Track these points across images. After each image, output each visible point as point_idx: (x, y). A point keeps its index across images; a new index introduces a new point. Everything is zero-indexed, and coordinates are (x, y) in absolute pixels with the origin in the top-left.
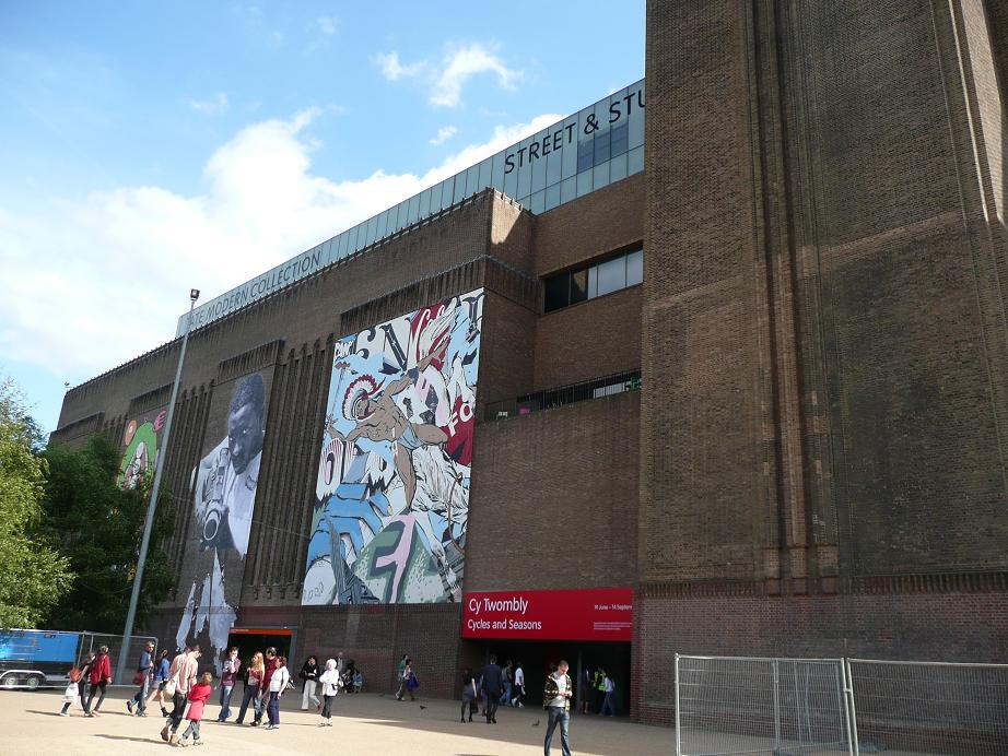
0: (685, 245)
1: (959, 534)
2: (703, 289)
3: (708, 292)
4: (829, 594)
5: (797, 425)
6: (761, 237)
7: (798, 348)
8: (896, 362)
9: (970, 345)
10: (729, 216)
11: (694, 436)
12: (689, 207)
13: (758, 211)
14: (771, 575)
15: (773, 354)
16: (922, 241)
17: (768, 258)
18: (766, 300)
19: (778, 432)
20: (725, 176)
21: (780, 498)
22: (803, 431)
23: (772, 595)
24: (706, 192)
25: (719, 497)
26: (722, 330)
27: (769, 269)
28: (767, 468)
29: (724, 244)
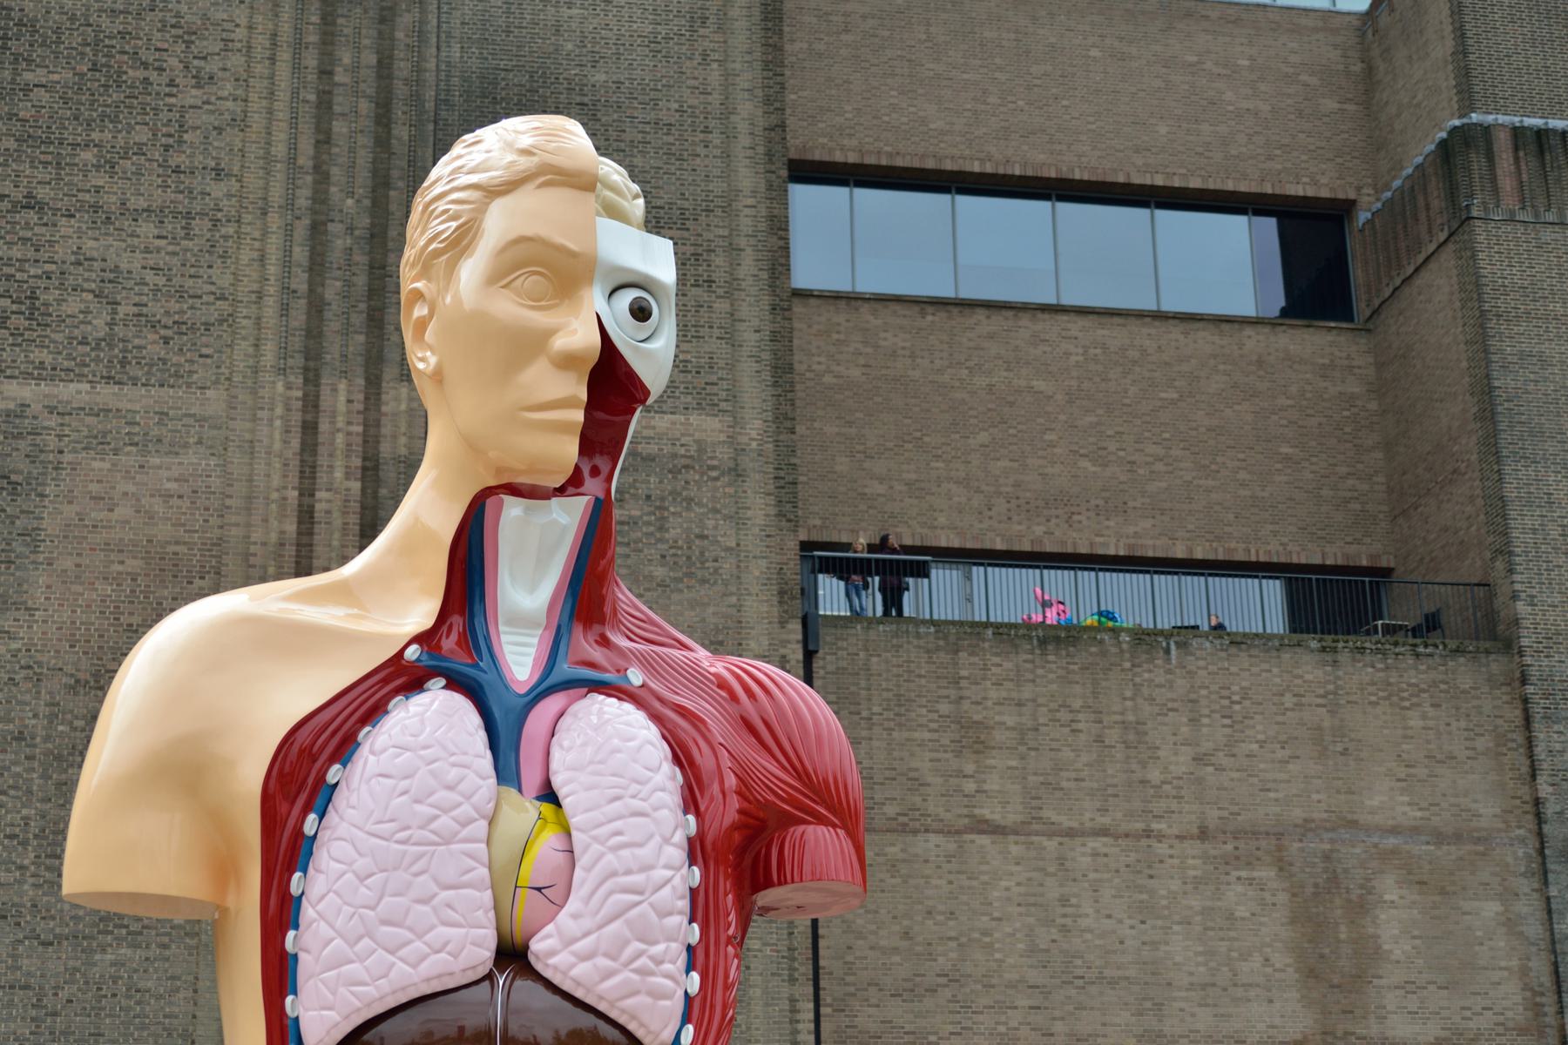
0: (62, 252)
2: (107, 394)
3: (124, 405)
6: (299, 317)
10: (200, 226)
11: (45, 776)
12: (88, 156)
13: (297, 250)
16: (651, 459)
17: (312, 378)
18: (294, 479)
20: (205, 118)
24: (142, 135)
25: (104, 951)
26: (151, 516)
27: (311, 403)
29: (181, 294)
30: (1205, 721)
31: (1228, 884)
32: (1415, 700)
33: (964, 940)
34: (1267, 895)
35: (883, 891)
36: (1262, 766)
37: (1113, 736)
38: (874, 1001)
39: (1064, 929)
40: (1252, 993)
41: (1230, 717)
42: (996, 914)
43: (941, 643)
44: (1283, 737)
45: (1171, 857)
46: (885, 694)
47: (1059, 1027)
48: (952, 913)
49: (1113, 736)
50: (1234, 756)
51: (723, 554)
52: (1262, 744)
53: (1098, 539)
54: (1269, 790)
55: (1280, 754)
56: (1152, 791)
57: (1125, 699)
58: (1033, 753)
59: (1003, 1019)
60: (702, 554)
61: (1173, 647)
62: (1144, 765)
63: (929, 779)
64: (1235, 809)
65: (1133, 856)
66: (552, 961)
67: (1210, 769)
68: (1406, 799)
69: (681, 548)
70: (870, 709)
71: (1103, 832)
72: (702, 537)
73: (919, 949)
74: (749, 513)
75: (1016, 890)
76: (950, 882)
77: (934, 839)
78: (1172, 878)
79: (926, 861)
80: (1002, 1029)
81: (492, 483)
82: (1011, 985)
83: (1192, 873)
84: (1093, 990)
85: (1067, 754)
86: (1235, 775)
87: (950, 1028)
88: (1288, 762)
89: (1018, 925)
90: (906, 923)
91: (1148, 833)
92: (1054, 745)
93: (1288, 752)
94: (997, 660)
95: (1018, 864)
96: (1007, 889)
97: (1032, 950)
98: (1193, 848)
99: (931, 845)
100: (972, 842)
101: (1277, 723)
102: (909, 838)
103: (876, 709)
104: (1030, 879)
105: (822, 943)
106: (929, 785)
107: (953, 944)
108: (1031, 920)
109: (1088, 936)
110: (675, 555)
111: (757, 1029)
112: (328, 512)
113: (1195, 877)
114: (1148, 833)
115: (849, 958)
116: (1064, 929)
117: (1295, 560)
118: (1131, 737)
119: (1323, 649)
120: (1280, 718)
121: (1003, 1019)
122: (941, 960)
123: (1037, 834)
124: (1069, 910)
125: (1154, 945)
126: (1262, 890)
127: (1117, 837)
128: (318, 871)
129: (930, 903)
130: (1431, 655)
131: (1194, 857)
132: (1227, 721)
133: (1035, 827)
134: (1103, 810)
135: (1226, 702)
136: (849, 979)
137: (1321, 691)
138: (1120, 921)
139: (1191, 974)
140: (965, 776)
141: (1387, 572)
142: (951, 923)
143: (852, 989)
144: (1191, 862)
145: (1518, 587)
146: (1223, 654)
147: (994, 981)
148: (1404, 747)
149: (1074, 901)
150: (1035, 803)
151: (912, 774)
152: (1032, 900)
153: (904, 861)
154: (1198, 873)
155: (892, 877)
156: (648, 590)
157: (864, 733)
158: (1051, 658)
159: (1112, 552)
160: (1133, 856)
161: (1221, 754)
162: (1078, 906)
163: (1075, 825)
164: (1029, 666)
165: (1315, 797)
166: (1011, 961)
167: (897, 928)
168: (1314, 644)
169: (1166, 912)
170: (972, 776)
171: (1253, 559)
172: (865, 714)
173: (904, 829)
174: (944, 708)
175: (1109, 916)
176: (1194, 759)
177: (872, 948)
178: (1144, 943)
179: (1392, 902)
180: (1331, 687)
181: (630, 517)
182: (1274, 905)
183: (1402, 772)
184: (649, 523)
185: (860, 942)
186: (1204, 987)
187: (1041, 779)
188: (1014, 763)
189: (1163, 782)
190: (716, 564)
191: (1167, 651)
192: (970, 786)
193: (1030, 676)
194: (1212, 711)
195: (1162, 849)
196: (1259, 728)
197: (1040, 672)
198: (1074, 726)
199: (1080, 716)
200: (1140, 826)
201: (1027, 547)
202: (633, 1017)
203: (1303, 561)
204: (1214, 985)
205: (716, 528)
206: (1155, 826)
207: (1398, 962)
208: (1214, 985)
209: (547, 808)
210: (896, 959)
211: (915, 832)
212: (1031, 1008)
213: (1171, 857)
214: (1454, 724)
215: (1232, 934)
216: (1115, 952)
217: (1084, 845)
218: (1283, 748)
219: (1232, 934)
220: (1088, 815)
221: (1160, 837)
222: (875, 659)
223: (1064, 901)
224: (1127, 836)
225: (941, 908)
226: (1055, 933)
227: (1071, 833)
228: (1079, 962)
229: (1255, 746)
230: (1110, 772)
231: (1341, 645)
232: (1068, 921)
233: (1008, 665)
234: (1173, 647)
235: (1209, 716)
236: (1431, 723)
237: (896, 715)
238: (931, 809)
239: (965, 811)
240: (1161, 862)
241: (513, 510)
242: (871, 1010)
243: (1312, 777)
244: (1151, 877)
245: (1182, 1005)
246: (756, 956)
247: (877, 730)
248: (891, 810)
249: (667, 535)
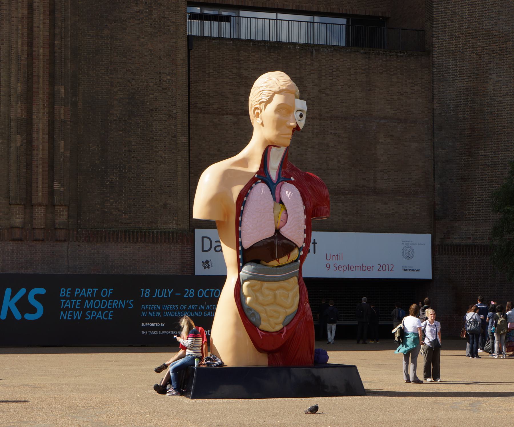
1: (148, 205)
4: (60, 241)
5: (47, 110)
7: (52, 46)
8: (120, 76)
9: (168, 77)
14: (17, 225)
15: (30, 44)
19: (30, 112)
21: (29, 166)
22: (51, 114)
23: (14, 240)
28: (17, 141)
30: (324, 78)
31: (328, 135)
32: (395, 72)
35: (212, 135)
41: (332, 77)
43: (234, 47)
48: (235, 143)
50: (333, 90)
51: (171, 24)
53: (286, 3)
54: (343, 103)
57: (296, 69)
60: (164, 24)
61: (314, 51)
66: (285, 233)
67: (324, 95)
68: (390, 107)
69: (157, 21)
70: (209, 70)
72: (164, 18)
74: (180, 9)
76: (235, 132)
77: (230, 117)
78: (309, 132)
79: (227, 125)
81: (271, 144)
83: (316, 131)
88: (350, 93)
94: (253, 54)
100: (243, 118)
101: (348, 79)
103: (211, 71)
106: (228, 98)
110: (155, 24)
111: (180, 185)
112: (38, 6)
113: (317, 132)
117: (355, 13)
119: (365, 53)
120: (349, 77)
126: (339, 137)
128: (245, 217)
130: (402, 56)
131: (317, 125)
132: (331, 78)
135: (331, 71)
137: (363, 68)
139: (313, 165)
140: (241, 95)
141: (387, 18)
144: (316, 127)
145: (434, 33)
146: (331, 54)
148: (390, 89)
155: (215, 130)
156: (146, 36)
158: (272, 54)
159: (291, 8)
161: (328, 89)
164: (264, 57)
165: (359, 105)
168: (362, 51)
169: (306, 144)
170: (243, 95)
171: (341, 12)
172: (207, 72)
174: (235, 71)
176: (319, 91)
177: (207, 154)
178: (298, 154)
179: (382, 142)
180: (367, 67)
181: (140, 10)
182: (343, 142)
184: (146, 12)
190: (169, 27)
191: (312, 53)
193: (264, 60)
194: (326, 74)
197: (268, 59)
201: (260, 6)
202: (297, 242)
203: (358, 13)
204: (321, 169)
205: (169, 14)
207: (382, 163)
208: (321, 169)
209: (281, 205)
211: (223, 114)
218: (349, 88)
222: (211, 53)
229: (340, 87)
231: (371, 52)
233: (257, 56)
234: (314, 51)
235: (325, 76)
236: (400, 80)
237: (219, 73)
241: (273, 149)
243: (358, 98)
246: (179, 162)
248: (215, 106)
249: (152, 17)
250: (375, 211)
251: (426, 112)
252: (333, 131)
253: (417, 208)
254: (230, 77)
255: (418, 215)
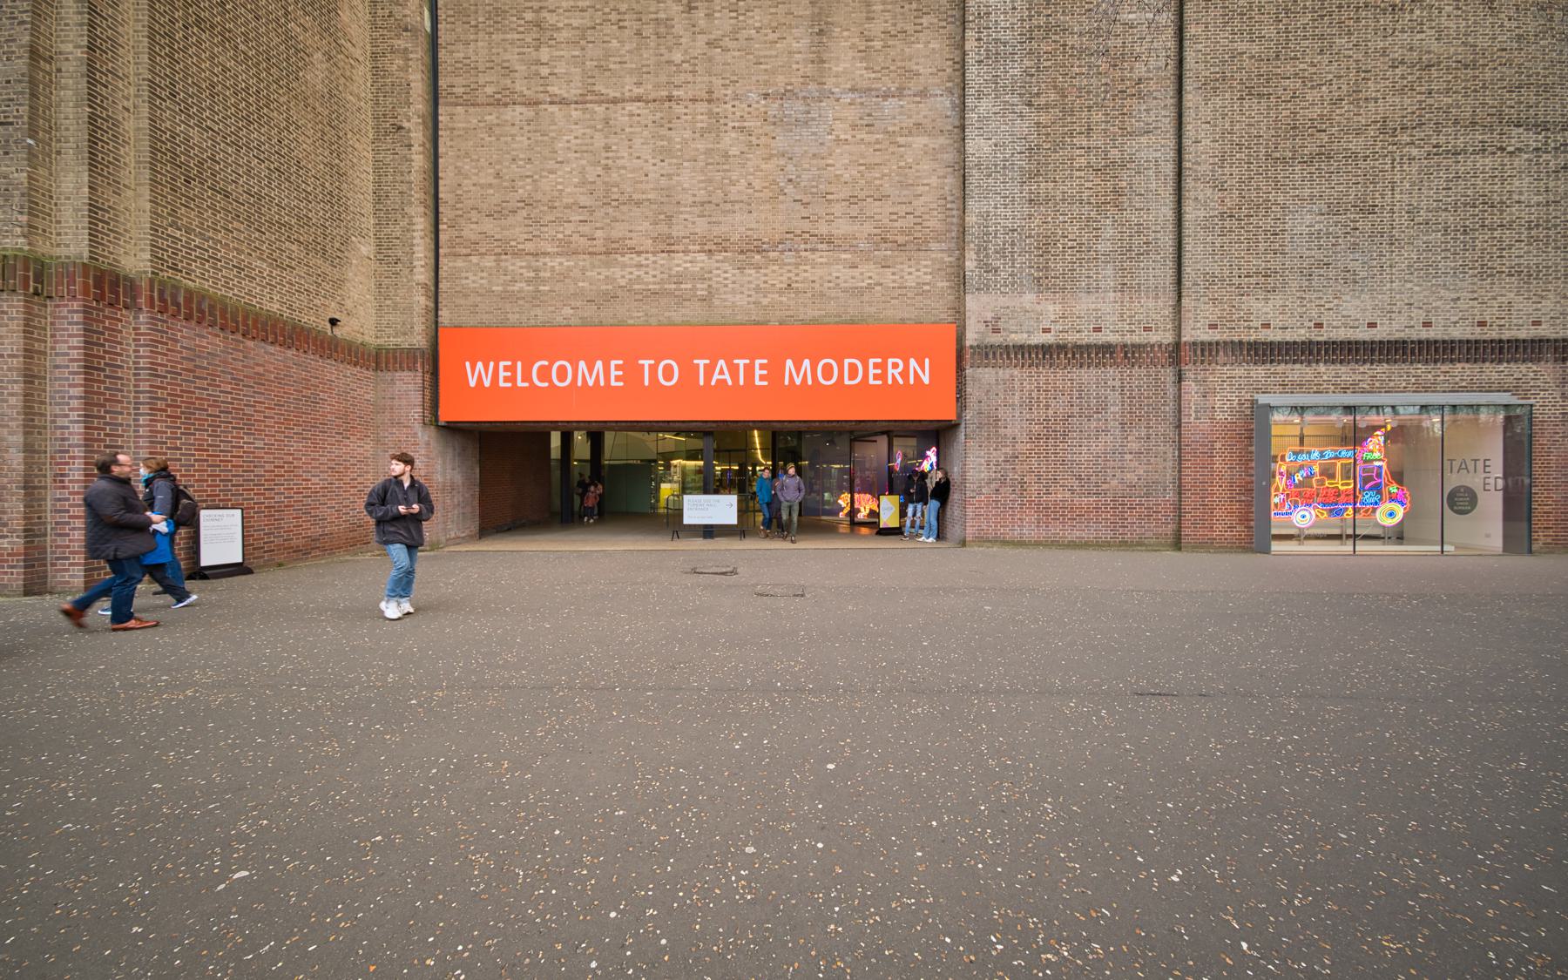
30: (717, 15)
31: (726, 132)
33: (536, 177)
34: (753, 139)
35: (483, 146)
36: (757, 46)
37: (648, 30)
38: (474, 220)
39: (607, 168)
40: (737, 207)
41: (736, 11)
42: (559, 159)
44: (774, 24)
45: (686, 114)
46: (487, 8)
47: (599, 234)
48: (529, 159)
49: (648, 30)
50: (737, 39)
52: (758, 30)
54: (761, 63)
55: (772, 37)
56: (675, 68)
58: (590, 45)
59: (561, 229)
62: (670, 50)
63: (517, 68)
64: (736, 78)
65: (659, 115)
70: (476, 19)
71: (639, 99)
73: (505, 184)
75: (574, 141)
76: (529, 139)
77: (519, 109)
78: (685, 129)
79: (513, 125)
80: (560, 236)
82: (567, 207)
83: (699, 125)
84: (624, 208)
85: (615, 43)
86: (737, 54)
87: (526, 236)
88: (777, 42)
89: (574, 166)
90: (497, 167)
91: (670, 98)
92: (606, 38)
93: (776, 36)
95: (577, 124)
96: (568, 141)
97: (583, 183)
98: (702, 107)
99: (517, 113)
100: (546, 110)
101: (771, 14)
102: (502, 109)
103: (480, 19)
104: (584, 134)
105: (441, 182)
106: (516, 71)
107: (529, 180)
108: (584, 162)
109: (623, 172)
111: (67, 129)
113: (702, 128)
114: (670, 98)
115: (459, 192)
116: (607, 168)
118: (662, 30)
120: (773, 10)
121: (561, 229)
122: (521, 191)
123: (591, 102)
124: (610, 154)
125: (670, 176)
126: (750, 135)
127: (647, 102)
129: (514, 153)
131: (702, 114)
132: (734, 14)
133: (589, 98)
134: (639, 84)
136: (458, 206)
138: (647, 161)
139: (694, 195)
140: (542, 64)
142: (528, 166)
143: (460, 212)
144: (700, 117)
147: (556, 204)
148: (866, 26)
149: (614, 148)
150: (590, 81)
151: (505, 65)
152: (585, 148)
153: (498, 125)
154: (704, 125)
155: (490, 136)
157: (472, 37)
160: (659, 115)
161: (727, 39)
162: (617, 151)
163: (618, 95)
166: (569, 190)
167: (491, 171)
169: (679, 154)
170: (547, 64)
172: (473, 23)
173: (498, 103)
174: (529, 16)
175: (639, 158)
176: (707, 44)
177: (474, 185)
178: (662, 175)
179: (846, 140)
182: (758, 145)
183: (862, 45)
185: (466, 181)
186: (702, 204)
187: (595, 63)
188: (577, 53)
189: (683, 62)
192: (545, 71)
194: (723, 8)
195: (679, 109)
196: (757, 18)
198: (621, 24)
199: (626, 17)
200: (665, 93)
204: (710, 202)
206: (675, 93)
207: (846, 183)
208: (710, 202)
210: (492, 191)
211: (506, 105)
212: (581, 221)
213: (686, 114)
214: (907, 6)
215: (725, 167)
216: (641, 182)
217: (624, 109)
218: (774, 32)
219: (725, 167)
220: (627, 87)
221: (679, 100)
223: (607, 148)
224: (654, 101)
225: (521, 156)
226: (599, 170)
227: (615, 101)
228: (615, 190)
230: (645, 56)
232: (610, 162)
235: (720, 11)
236: (889, 7)
237: (495, 22)
238: (518, 88)
239: (541, 89)
240: (678, 118)
242: (473, 226)
243: (794, 53)
244: (670, 129)
245: (686, 216)
246: (67, 59)
247: (481, 34)
248: (489, 90)
250: (830, 282)
251: (949, 70)
252: (737, 124)
253: (925, 274)
254: (522, 29)
255: (926, 288)
